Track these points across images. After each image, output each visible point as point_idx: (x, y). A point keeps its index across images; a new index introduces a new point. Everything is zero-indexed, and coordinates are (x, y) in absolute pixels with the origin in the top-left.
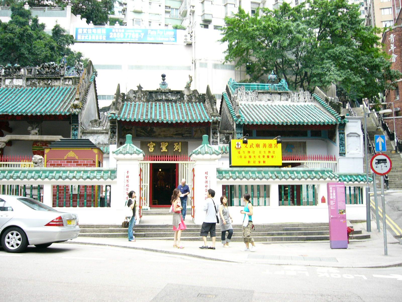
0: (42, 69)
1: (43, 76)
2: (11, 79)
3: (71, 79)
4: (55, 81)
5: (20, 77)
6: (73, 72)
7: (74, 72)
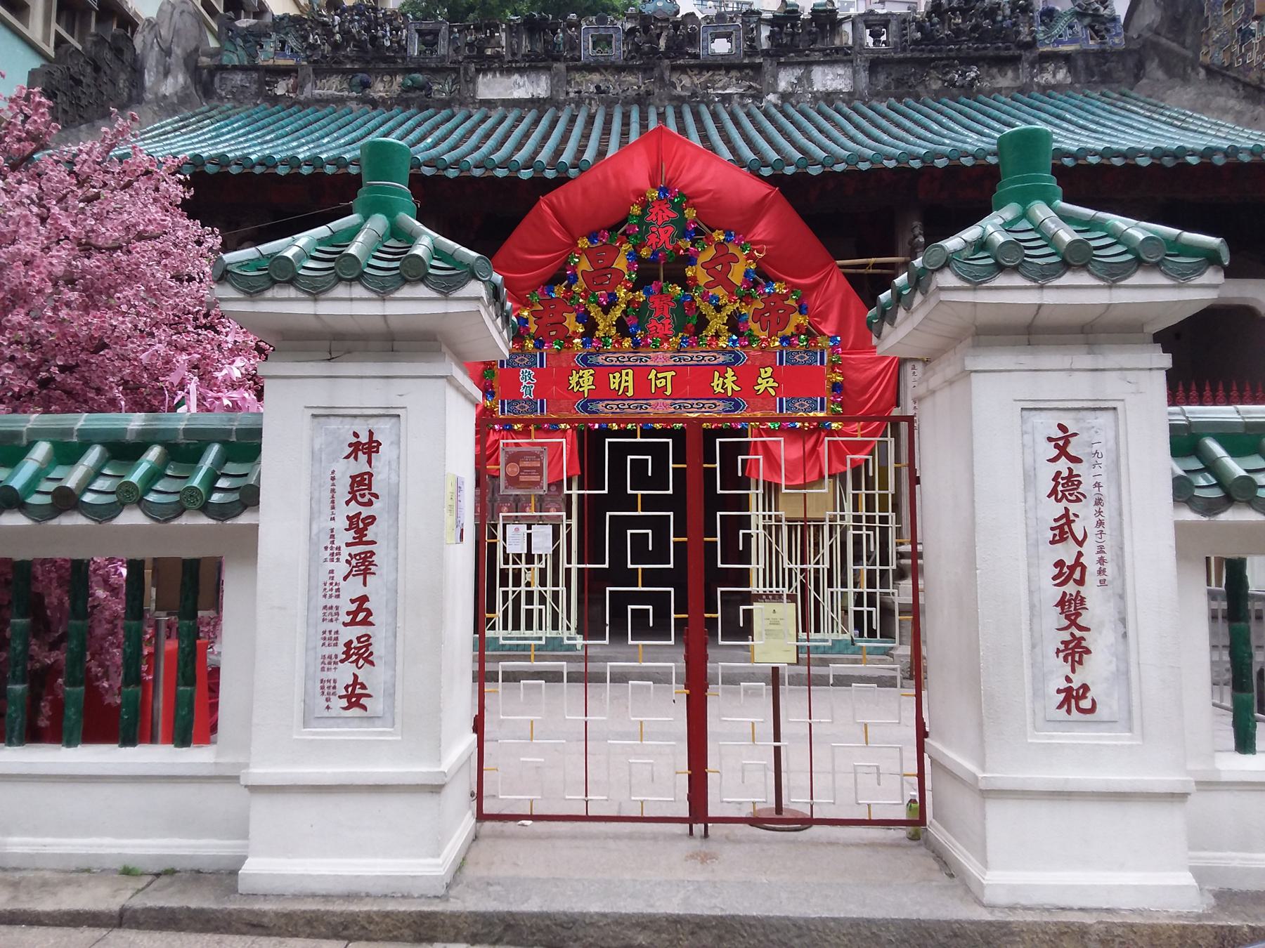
0: (936, 20)
1: (940, 51)
2: (799, 64)
3: (1067, 58)
4: (994, 71)
5: (840, 56)
6: (1071, 27)
7: (1078, 28)
